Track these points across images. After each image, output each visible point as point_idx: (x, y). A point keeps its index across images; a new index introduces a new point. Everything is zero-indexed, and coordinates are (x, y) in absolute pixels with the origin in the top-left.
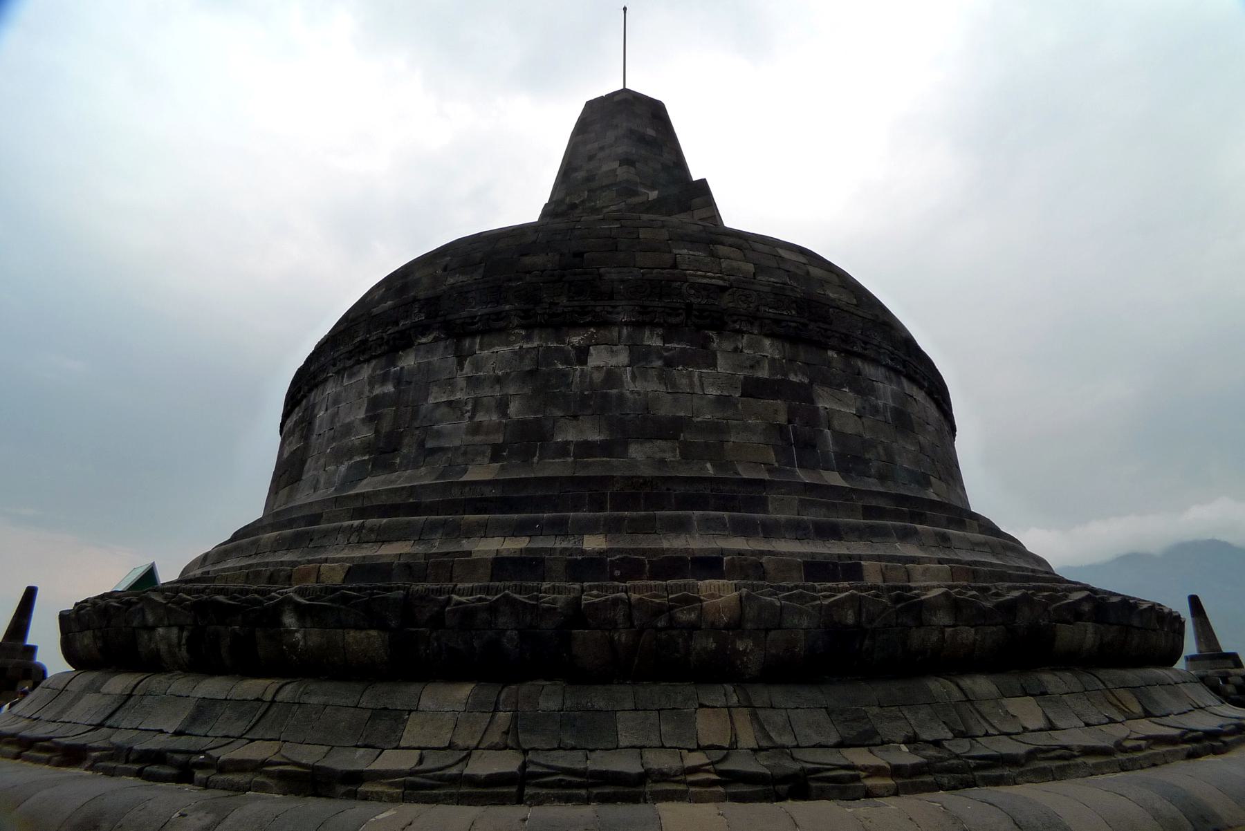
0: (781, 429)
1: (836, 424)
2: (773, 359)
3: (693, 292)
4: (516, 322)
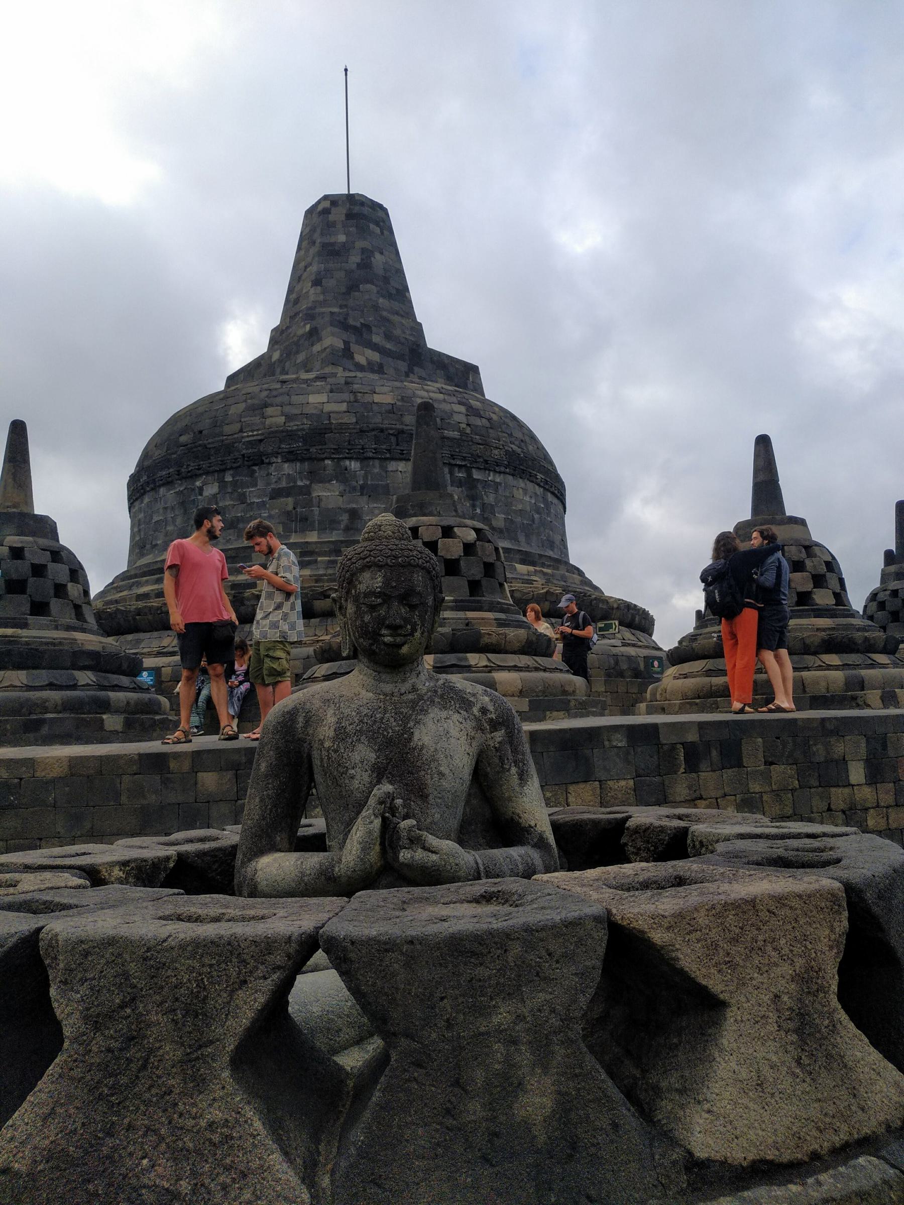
0: (288, 513)
1: (323, 505)
2: (289, 474)
3: (244, 447)
4: (177, 477)
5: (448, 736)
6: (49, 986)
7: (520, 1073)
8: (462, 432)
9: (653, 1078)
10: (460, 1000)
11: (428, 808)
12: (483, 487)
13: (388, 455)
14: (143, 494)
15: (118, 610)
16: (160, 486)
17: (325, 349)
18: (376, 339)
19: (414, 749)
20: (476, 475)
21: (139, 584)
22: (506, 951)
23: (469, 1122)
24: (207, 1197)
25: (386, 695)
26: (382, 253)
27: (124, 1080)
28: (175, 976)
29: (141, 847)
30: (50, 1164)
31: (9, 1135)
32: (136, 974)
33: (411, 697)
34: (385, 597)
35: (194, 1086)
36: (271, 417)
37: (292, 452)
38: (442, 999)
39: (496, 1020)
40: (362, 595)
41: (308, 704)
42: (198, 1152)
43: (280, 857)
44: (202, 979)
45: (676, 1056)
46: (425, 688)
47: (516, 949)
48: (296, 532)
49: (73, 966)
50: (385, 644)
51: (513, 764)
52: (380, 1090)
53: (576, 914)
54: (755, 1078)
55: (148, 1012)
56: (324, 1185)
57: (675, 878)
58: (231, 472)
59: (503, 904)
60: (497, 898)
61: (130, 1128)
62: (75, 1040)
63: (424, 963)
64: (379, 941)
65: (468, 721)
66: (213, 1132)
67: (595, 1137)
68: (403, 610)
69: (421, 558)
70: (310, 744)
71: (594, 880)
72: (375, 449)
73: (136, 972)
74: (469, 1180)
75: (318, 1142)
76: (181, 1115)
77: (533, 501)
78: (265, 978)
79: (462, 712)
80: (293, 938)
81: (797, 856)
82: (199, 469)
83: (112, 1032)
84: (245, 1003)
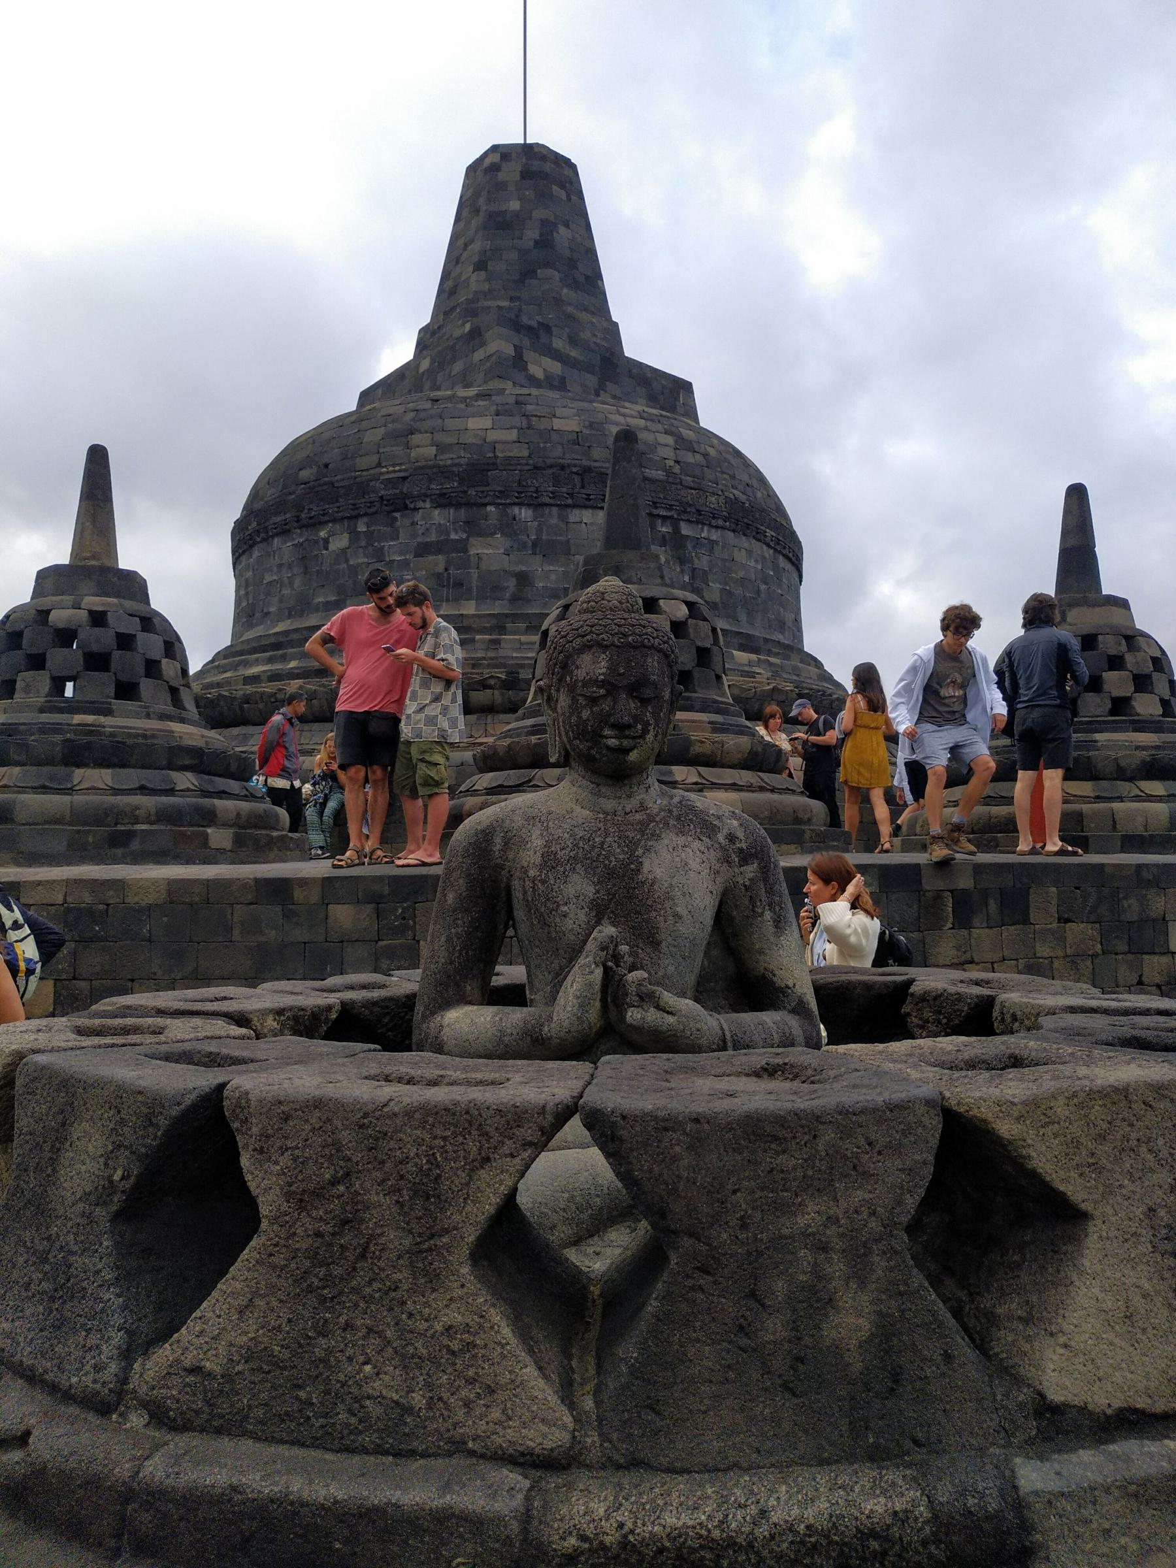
0: (438, 576)
1: (483, 566)
2: (440, 524)
4: (296, 524)
5: (687, 868)
6: (238, 1155)
7: (830, 1286)
8: (669, 472)
9: (986, 1303)
10: (758, 1194)
11: (659, 959)
12: (694, 547)
13: (570, 501)
14: (251, 546)
15: (220, 695)
16: (273, 537)
17: (490, 356)
18: (558, 344)
19: (643, 883)
20: (685, 530)
21: (246, 664)
22: (815, 1137)
23: (769, 1343)
24: (446, 1413)
25: (606, 813)
26: (567, 226)
27: (337, 1271)
28: (400, 1148)
29: (292, 993)
30: (251, 1365)
31: (197, 1329)
32: (350, 1145)
33: (638, 817)
34: (610, 687)
35: (426, 1282)
36: (418, 447)
37: (445, 494)
38: (735, 1192)
39: (801, 1221)
40: (580, 684)
41: (508, 821)
42: (434, 1360)
43: (471, 1011)
44: (434, 1154)
45: (1018, 1276)
46: (655, 806)
47: (828, 1135)
48: (448, 600)
49: (270, 1132)
50: (608, 748)
51: (767, 908)
52: (656, 1299)
53: (903, 1095)
54: (1123, 1308)
55: (367, 1191)
56: (587, 1408)
57: (1010, 1057)
58: (365, 519)
59: (791, 1080)
60: (783, 1072)
61: (347, 1327)
62: (274, 1220)
63: (712, 1147)
64: (656, 1117)
65: (711, 850)
66: (451, 1338)
67: (922, 1369)
68: (633, 705)
69: (658, 637)
70: (509, 872)
71: (906, 1055)
72: (552, 493)
73: (350, 1141)
74: (767, 1411)
75: (569, 1357)
76: (410, 1315)
77: (760, 567)
78: (512, 1156)
79: (704, 838)
80: (548, 1109)
81: (1158, 1036)
82: (324, 515)
83: (321, 1213)
84: (489, 1186)
